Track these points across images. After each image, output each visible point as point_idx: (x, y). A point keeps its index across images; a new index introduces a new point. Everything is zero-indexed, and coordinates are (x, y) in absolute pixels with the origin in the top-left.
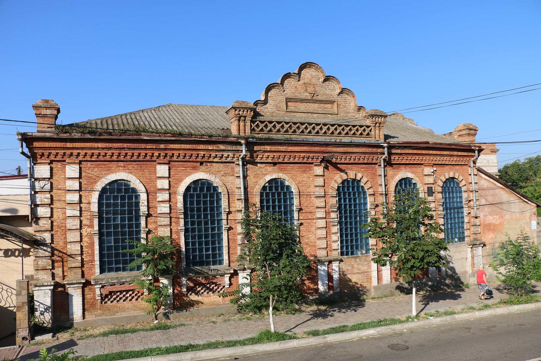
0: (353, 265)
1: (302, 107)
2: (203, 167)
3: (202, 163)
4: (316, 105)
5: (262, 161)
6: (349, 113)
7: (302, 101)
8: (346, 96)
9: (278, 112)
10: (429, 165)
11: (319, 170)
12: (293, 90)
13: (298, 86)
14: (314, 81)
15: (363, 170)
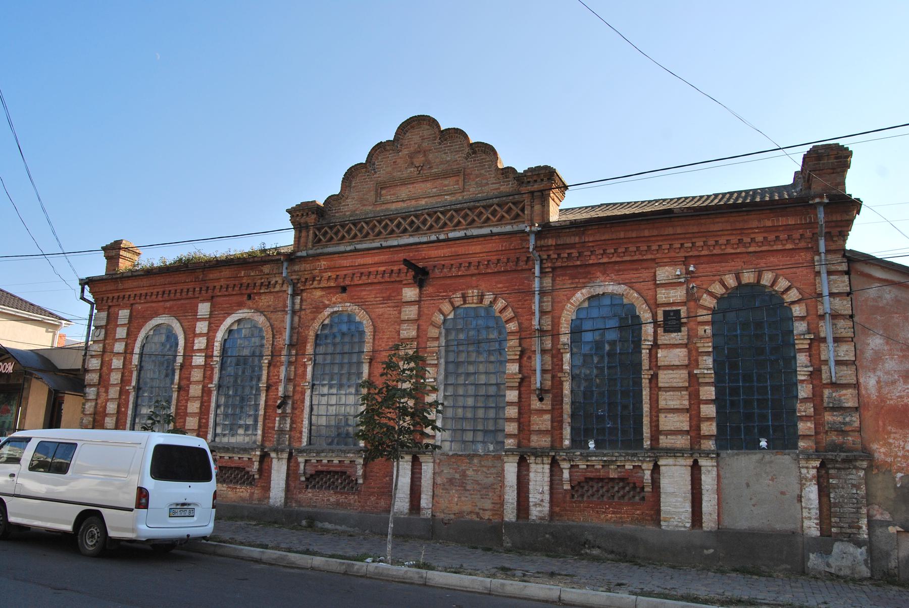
0: (464, 472)
1: (404, 192)
2: (250, 303)
3: (249, 297)
4: (429, 185)
5: (321, 286)
6: (487, 184)
7: (404, 182)
8: (484, 156)
9: (364, 208)
10: (673, 262)
11: (410, 293)
12: (389, 169)
13: (399, 161)
14: (425, 145)
15: (500, 285)
